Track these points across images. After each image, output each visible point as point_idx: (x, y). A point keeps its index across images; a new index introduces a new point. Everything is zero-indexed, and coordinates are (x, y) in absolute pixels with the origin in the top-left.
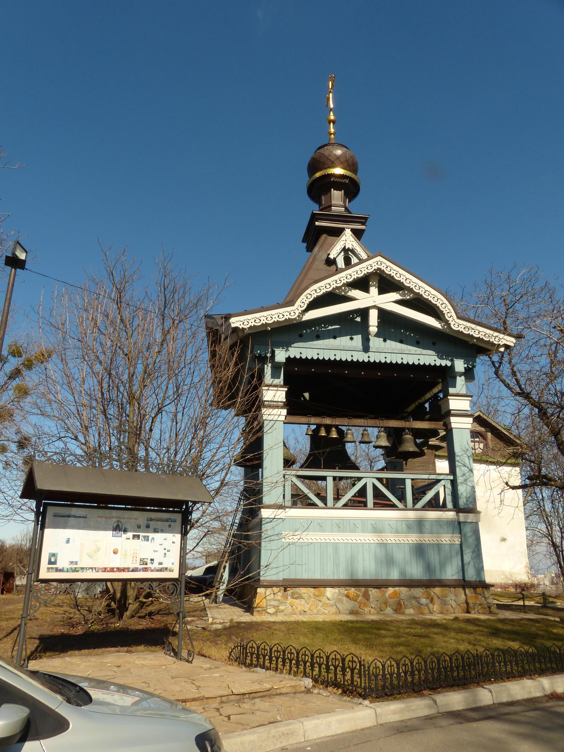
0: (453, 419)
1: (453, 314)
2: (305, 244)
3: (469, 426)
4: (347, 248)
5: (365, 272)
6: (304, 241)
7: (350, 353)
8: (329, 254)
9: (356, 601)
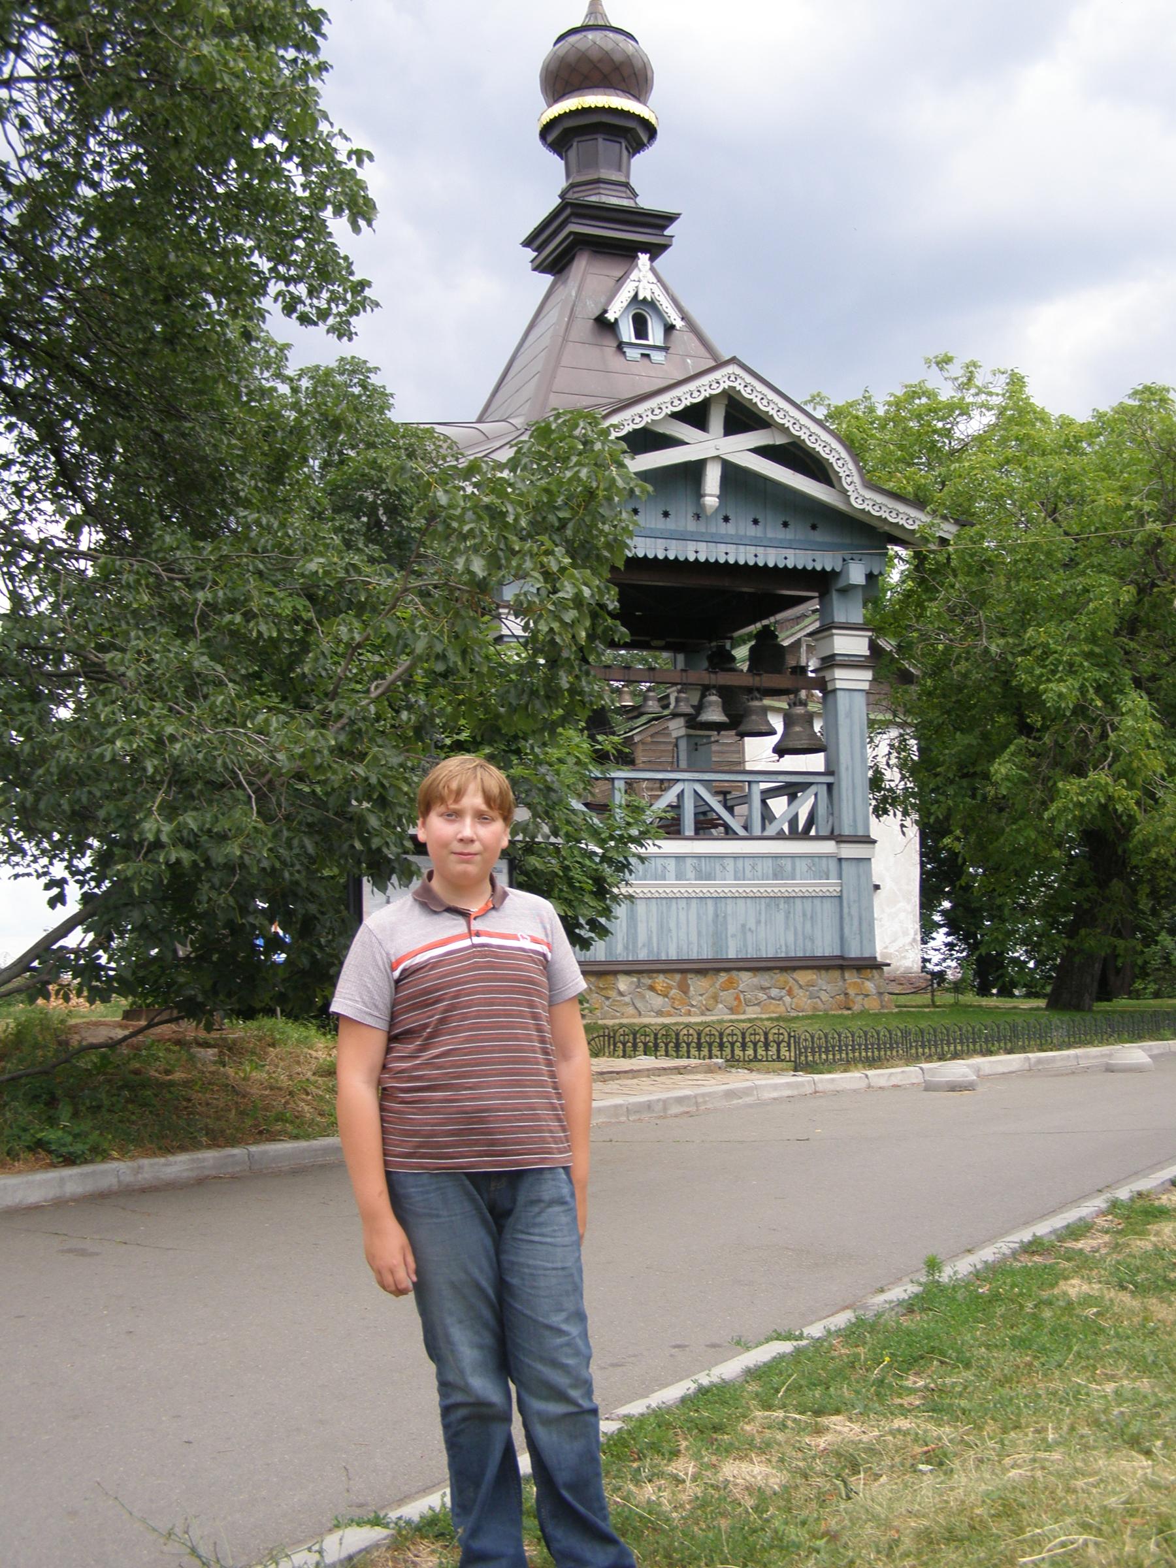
0: (839, 673)
1: (856, 478)
2: (530, 254)
3: (866, 686)
4: (641, 297)
5: (705, 394)
6: (527, 243)
7: (661, 543)
8: (605, 311)
9: (666, 996)
